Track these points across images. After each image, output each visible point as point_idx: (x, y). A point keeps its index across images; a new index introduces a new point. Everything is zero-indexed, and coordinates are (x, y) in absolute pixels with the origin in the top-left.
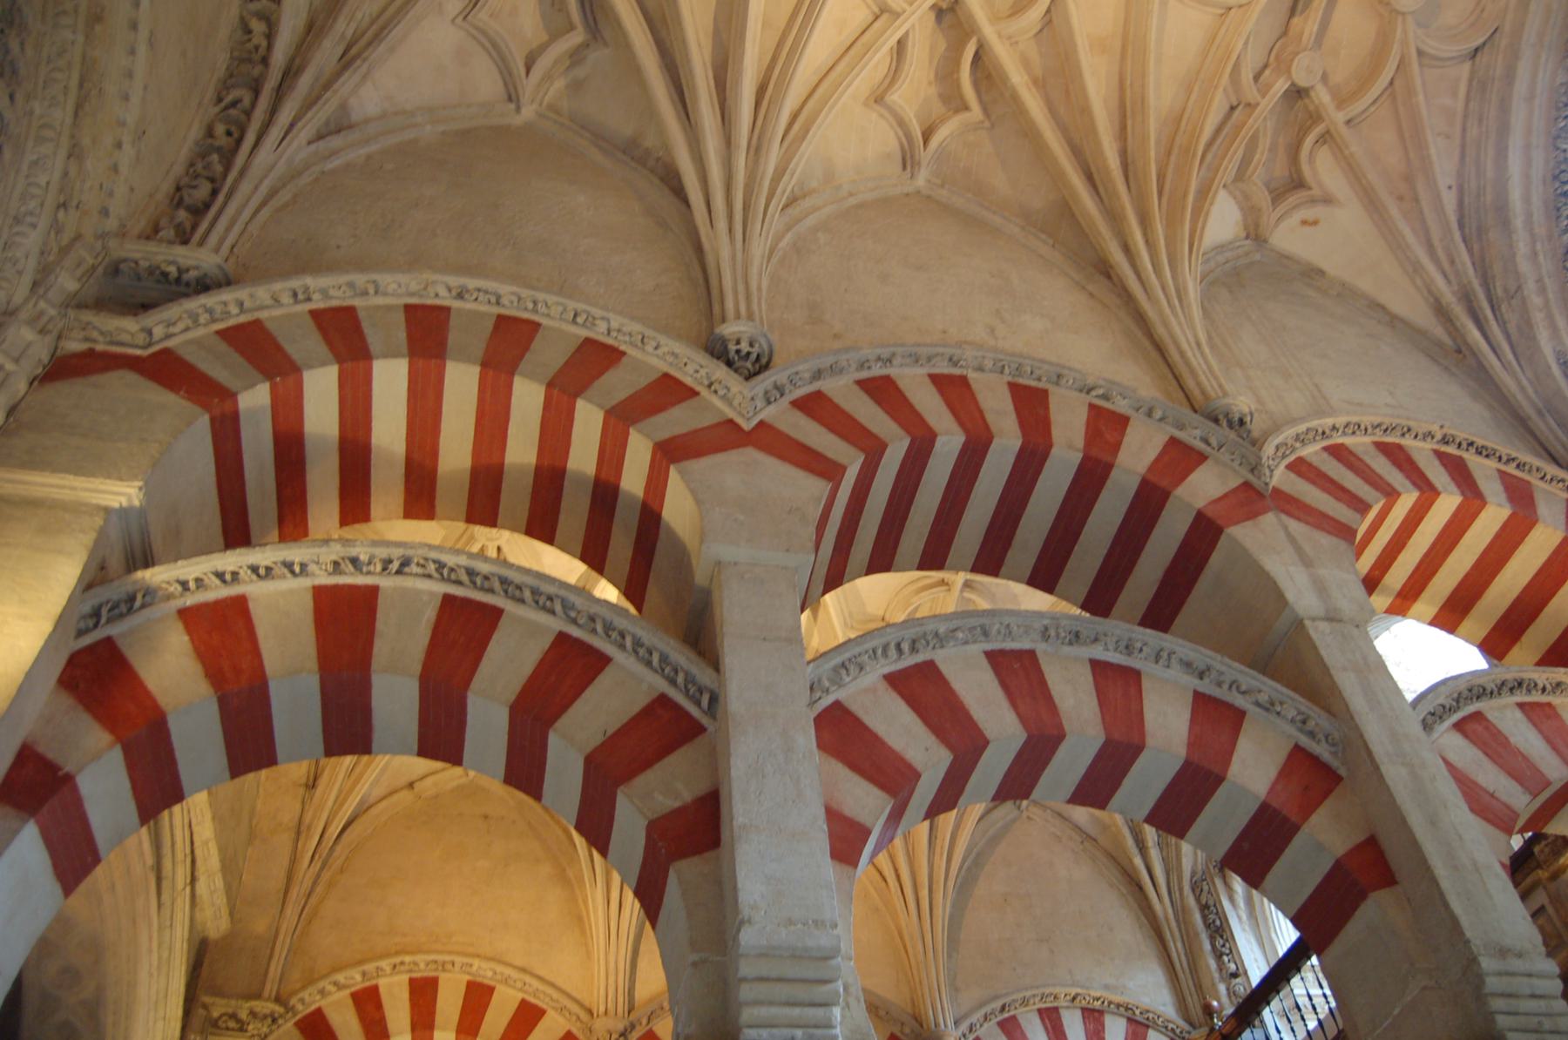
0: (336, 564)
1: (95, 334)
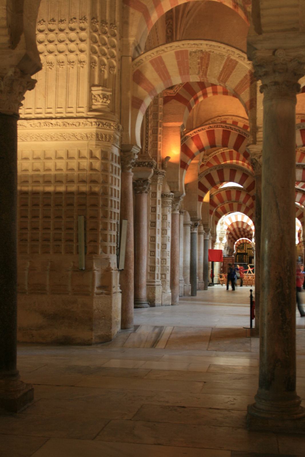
0: (208, 127)
1: (168, 93)
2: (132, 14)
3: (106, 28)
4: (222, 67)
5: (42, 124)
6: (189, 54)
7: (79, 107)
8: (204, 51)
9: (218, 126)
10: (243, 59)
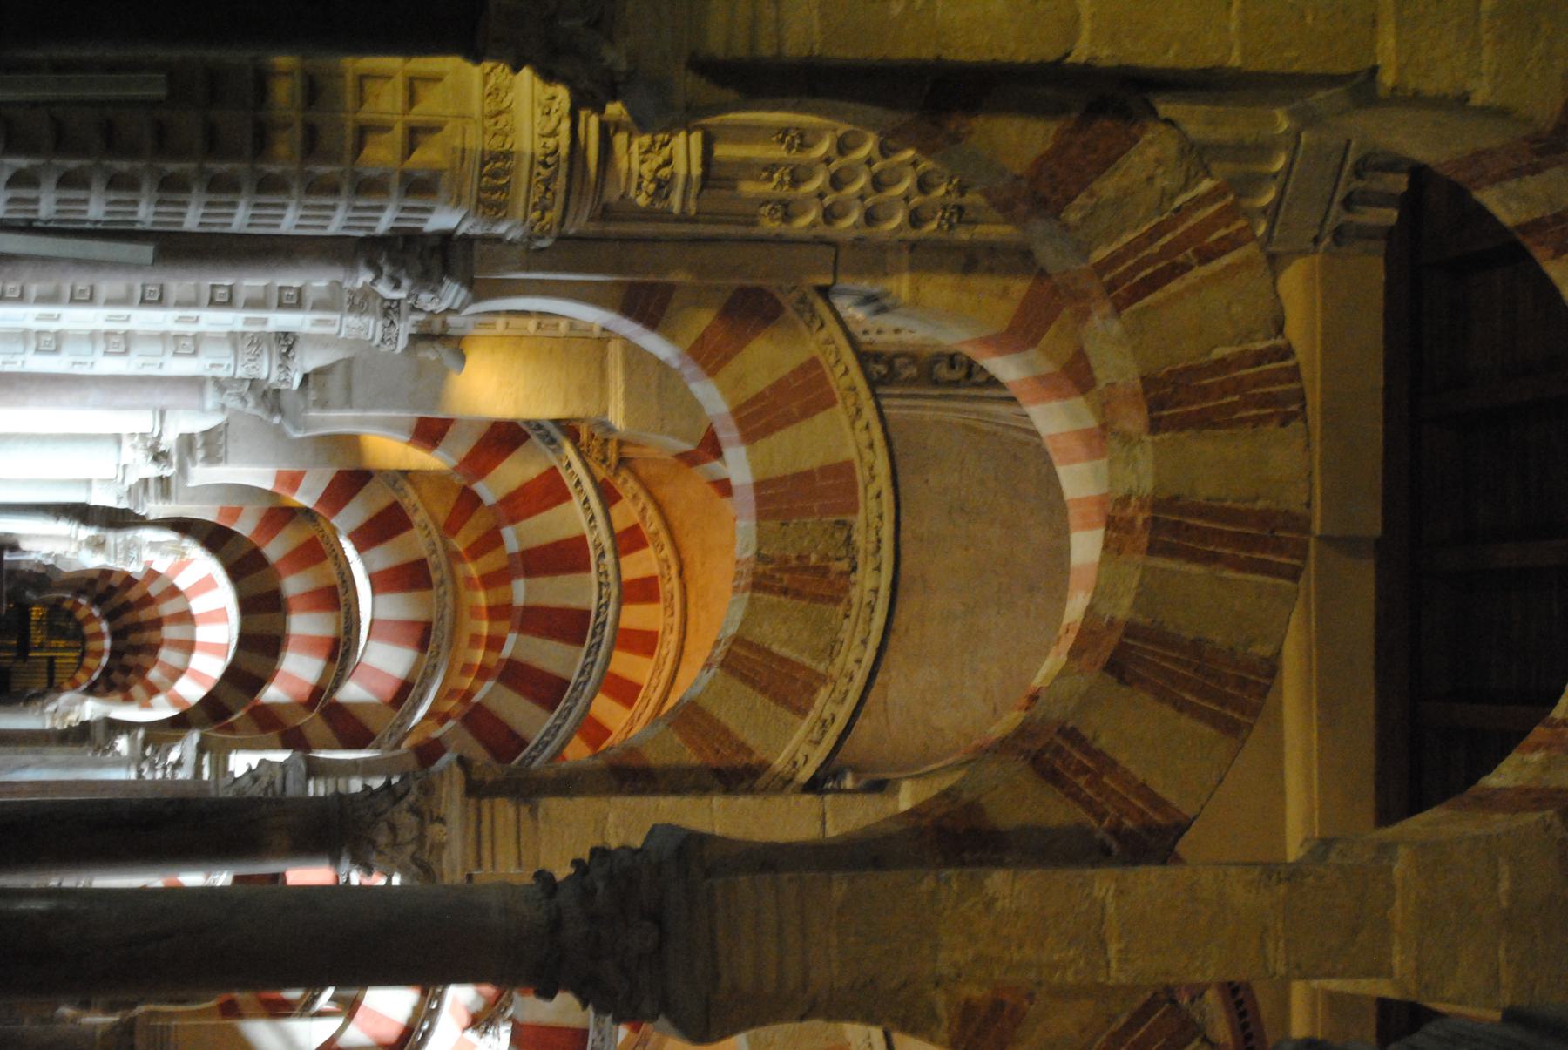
2: (1005, 291)
3: (941, 191)
4: (786, 652)
6: (842, 518)
8: (853, 577)
9: (604, 590)
10: (815, 736)
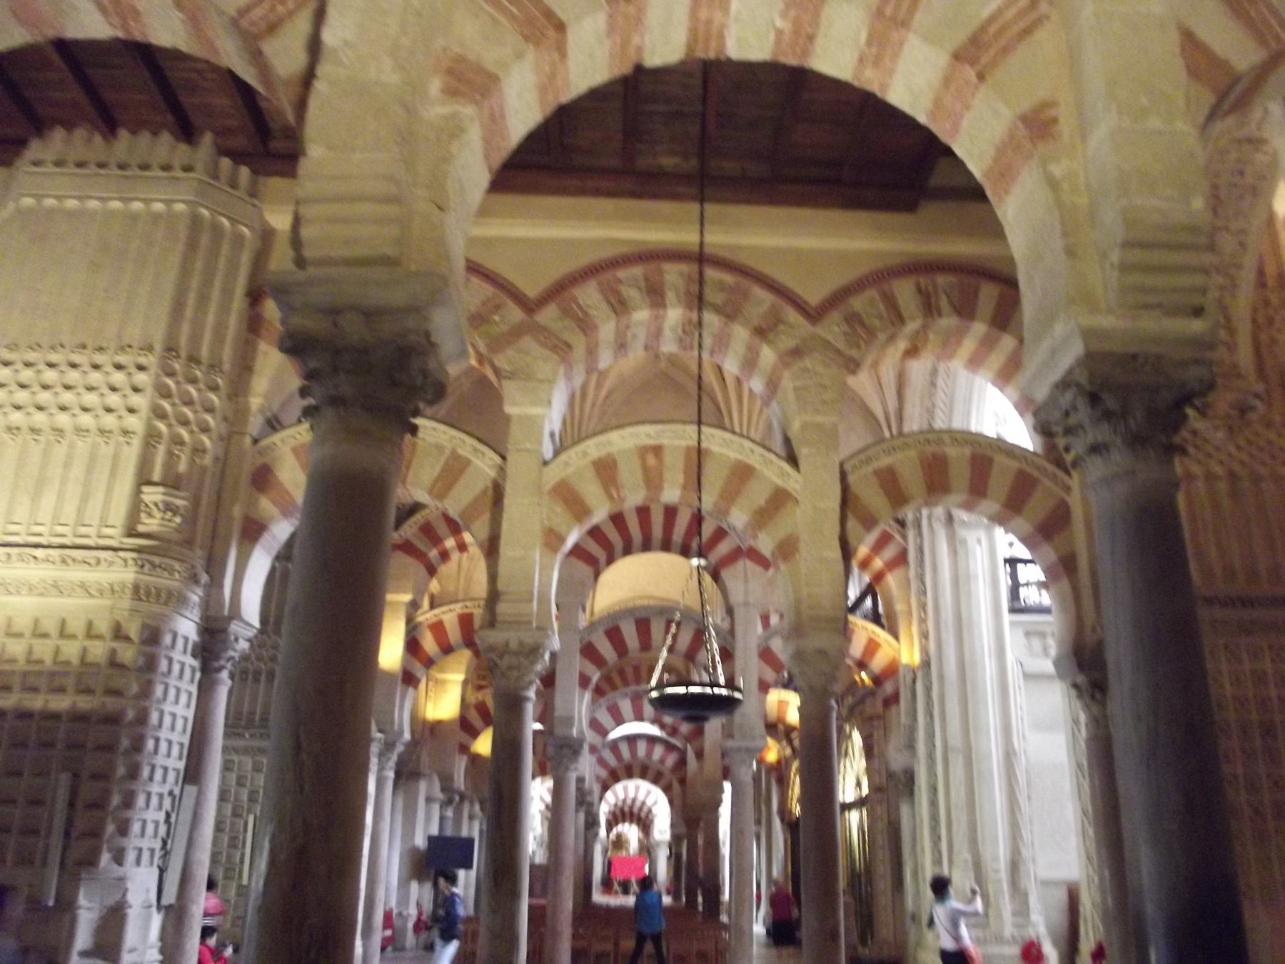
5: (14, 558)
7: (107, 526)
